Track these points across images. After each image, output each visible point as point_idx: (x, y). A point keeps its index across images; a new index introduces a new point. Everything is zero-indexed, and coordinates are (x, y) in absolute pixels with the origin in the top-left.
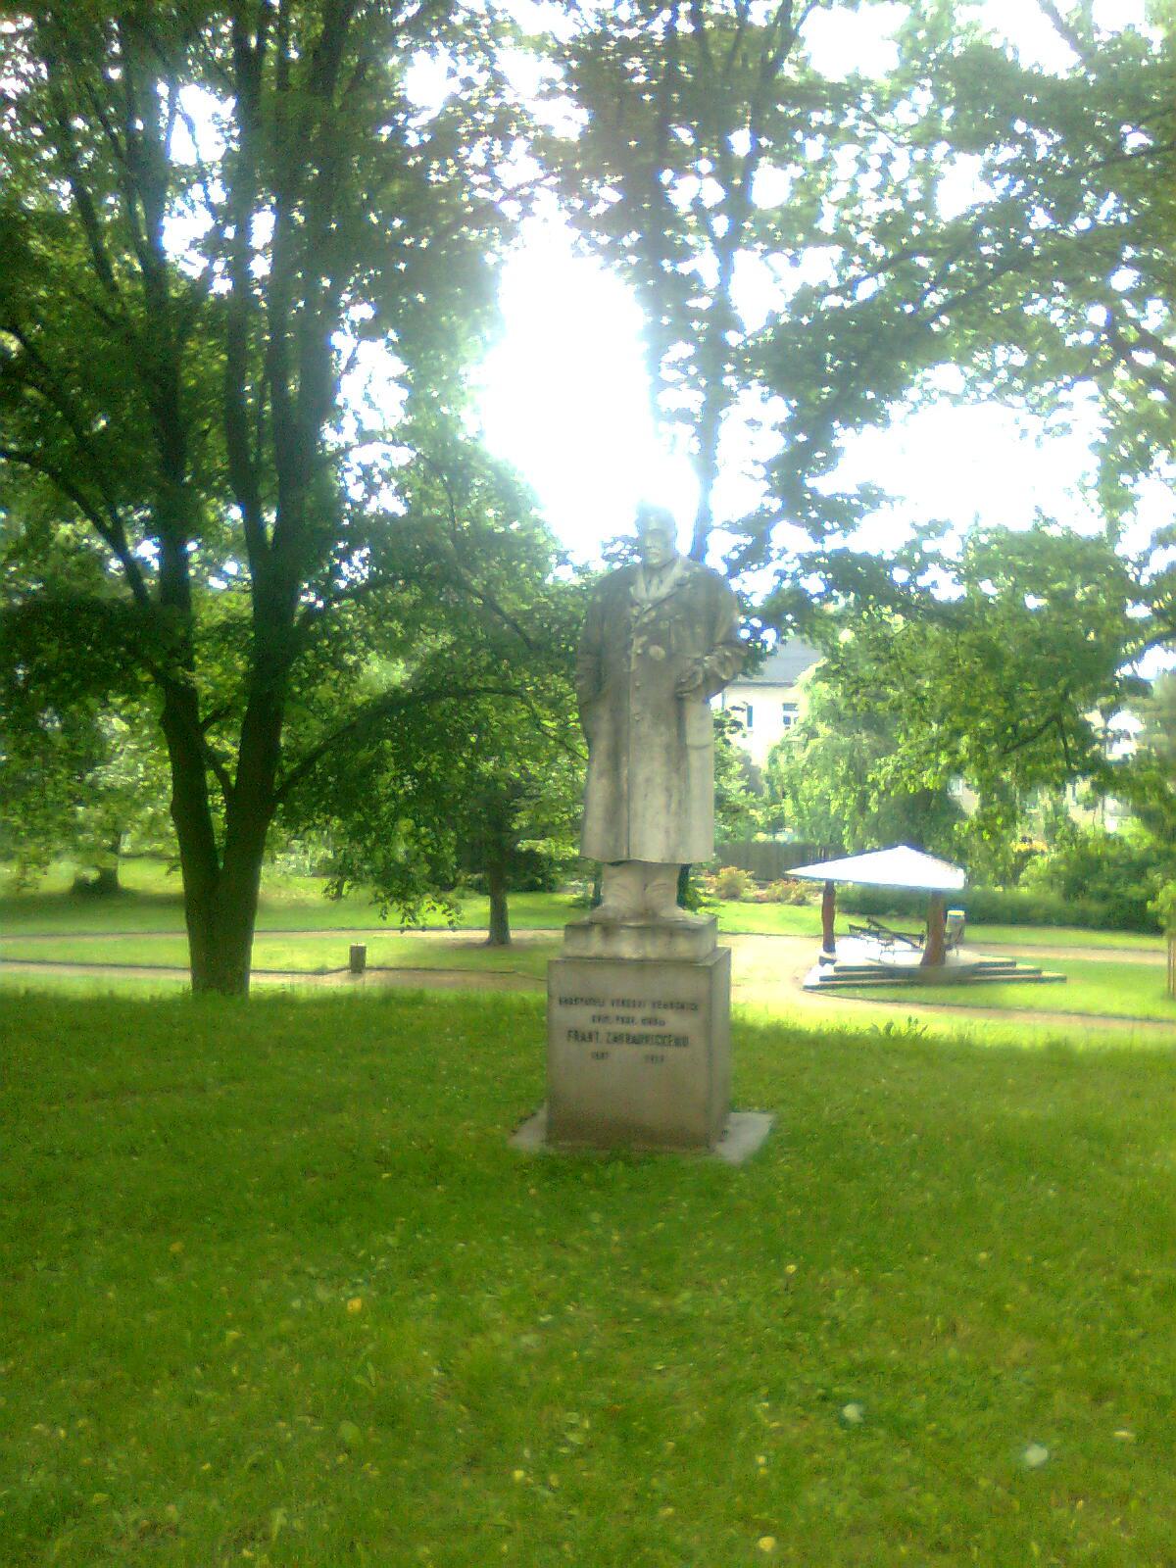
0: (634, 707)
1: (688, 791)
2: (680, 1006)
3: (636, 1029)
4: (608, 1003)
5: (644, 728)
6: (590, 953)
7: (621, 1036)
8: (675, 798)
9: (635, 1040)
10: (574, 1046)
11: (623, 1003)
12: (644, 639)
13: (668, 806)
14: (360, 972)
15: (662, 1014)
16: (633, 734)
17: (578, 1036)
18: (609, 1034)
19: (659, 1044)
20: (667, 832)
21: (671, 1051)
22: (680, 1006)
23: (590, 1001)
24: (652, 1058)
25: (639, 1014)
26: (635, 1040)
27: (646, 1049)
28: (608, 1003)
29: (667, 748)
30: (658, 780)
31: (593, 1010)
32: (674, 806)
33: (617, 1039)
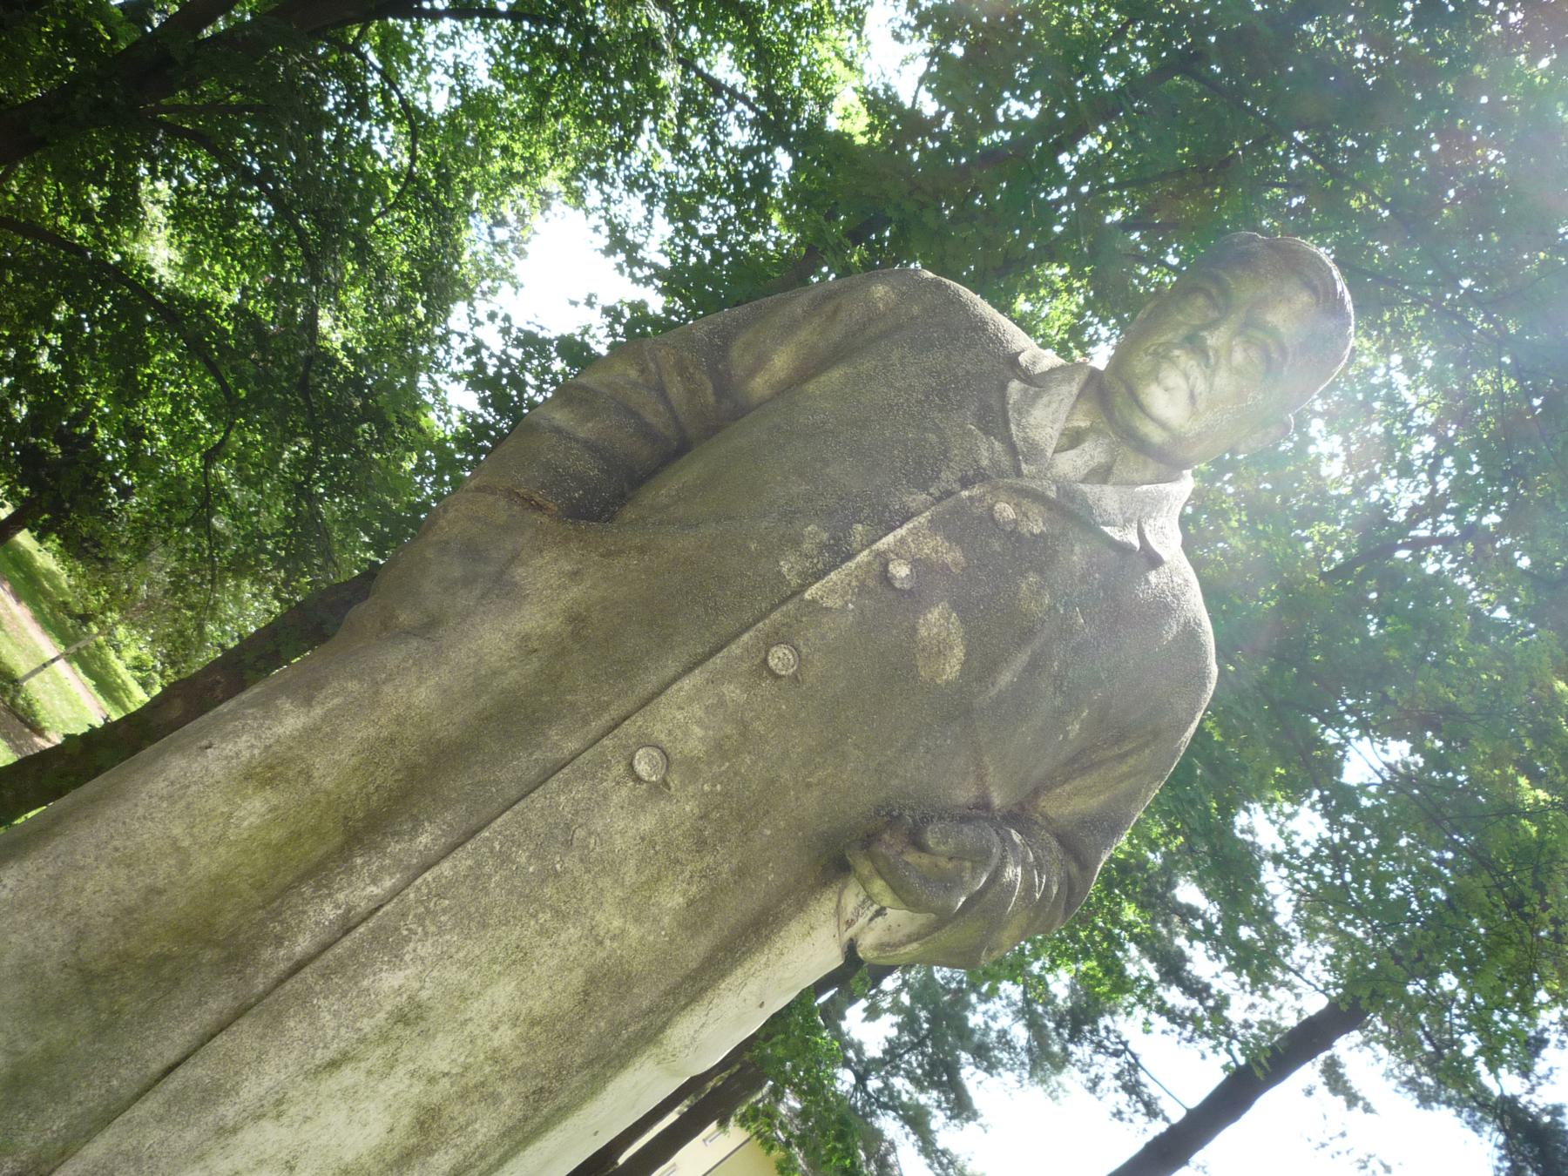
16: (562, 797)
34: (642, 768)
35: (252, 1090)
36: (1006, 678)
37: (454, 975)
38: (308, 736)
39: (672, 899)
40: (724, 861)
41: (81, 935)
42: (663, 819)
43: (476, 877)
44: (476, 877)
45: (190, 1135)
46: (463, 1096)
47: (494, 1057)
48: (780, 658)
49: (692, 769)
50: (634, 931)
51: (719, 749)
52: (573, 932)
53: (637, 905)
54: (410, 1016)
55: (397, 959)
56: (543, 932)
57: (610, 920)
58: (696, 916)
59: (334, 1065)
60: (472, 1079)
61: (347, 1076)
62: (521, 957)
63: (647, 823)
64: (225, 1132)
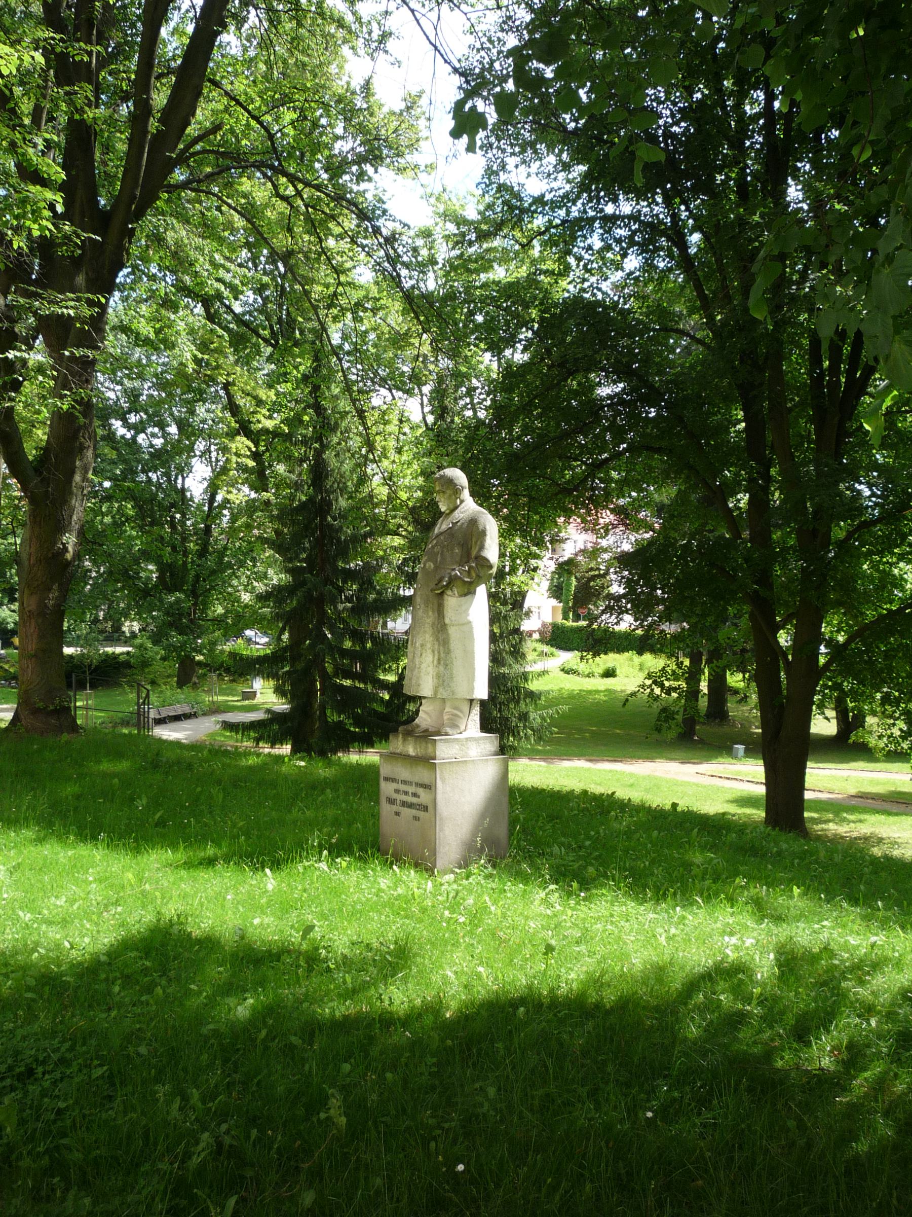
1: (448, 652)
3: (410, 799)
6: (398, 751)
9: (410, 806)
15: (420, 791)
17: (391, 801)
21: (421, 814)
23: (394, 780)
26: (410, 806)
27: (414, 812)
29: (433, 625)
30: (429, 645)
31: (394, 786)
33: (404, 804)
53: (428, 617)
54: (422, 645)
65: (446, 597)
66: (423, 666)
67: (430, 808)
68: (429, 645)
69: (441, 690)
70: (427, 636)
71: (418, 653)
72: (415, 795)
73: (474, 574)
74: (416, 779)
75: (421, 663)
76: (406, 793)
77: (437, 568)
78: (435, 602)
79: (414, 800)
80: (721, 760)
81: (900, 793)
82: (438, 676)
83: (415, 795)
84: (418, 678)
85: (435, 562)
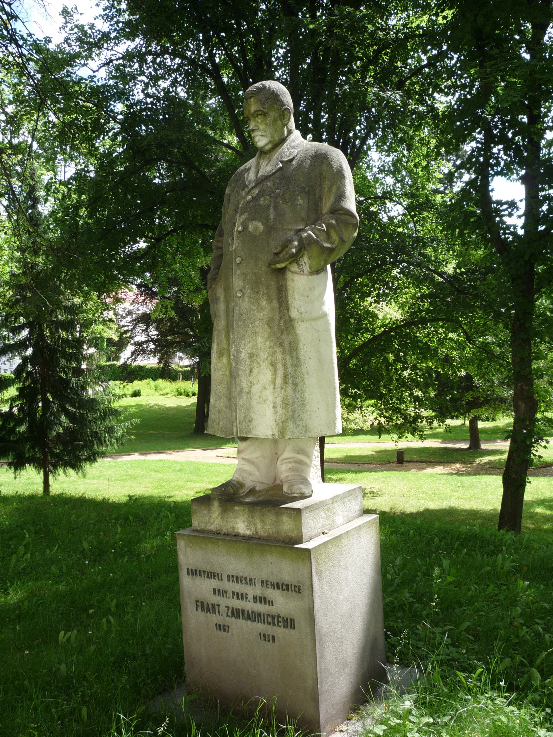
0: (237, 283)
1: (297, 364)
2: (286, 587)
3: (249, 606)
4: (225, 578)
5: (245, 304)
6: (213, 527)
7: (238, 610)
8: (280, 373)
9: (251, 616)
10: (201, 615)
11: (237, 579)
12: (245, 216)
13: (274, 381)
14: (402, 463)
18: (228, 607)
19: (269, 624)
20: (274, 407)
21: (279, 632)
22: (286, 587)
23: (211, 575)
24: (265, 637)
25: (251, 591)
26: (251, 616)
27: (261, 627)
28: (225, 578)
29: (270, 322)
30: (263, 355)
31: (213, 583)
32: (279, 381)
33: (236, 613)
34: (239, 295)
35: (244, 385)
36: (272, 216)
37: (250, 345)
38: (218, 345)
39: (264, 303)
40: (263, 290)
41: (226, 396)
42: (248, 297)
43: (238, 332)
44: (238, 332)
45: (244, 397)
46: (272, 356)
47: (270, 348)
48: (238, 260)
49: (244, 287)
50: (265, 312)
51: (244, 280)
52: (257, 323)
55: (241, 352)
56: (253, 327)
57: (260, 315)
58: (270, 300)
59: (251, 371)
60: (271, 353)
61: (255, 371)
62: (255, 333)
63: (247, 300)
64: (249, 393)
65: (289, 275)
66: (256, 389)
67: (300, 622)
68: (263, 355)
69: (290, 426)
70: (260, 340)
71: (243, 368)
72: (261, 600)
73: (335, 237)
74: (265, 575)
75: (251, 384)
76: (241, 596)
77: (269, 230)
78: (272, 283)
79: (260, 608)
80: (229, 445)
81: (353, 457)
82: (286, 404)
83: (261, 600)
84: (248, 409)
85: (265, 220)
